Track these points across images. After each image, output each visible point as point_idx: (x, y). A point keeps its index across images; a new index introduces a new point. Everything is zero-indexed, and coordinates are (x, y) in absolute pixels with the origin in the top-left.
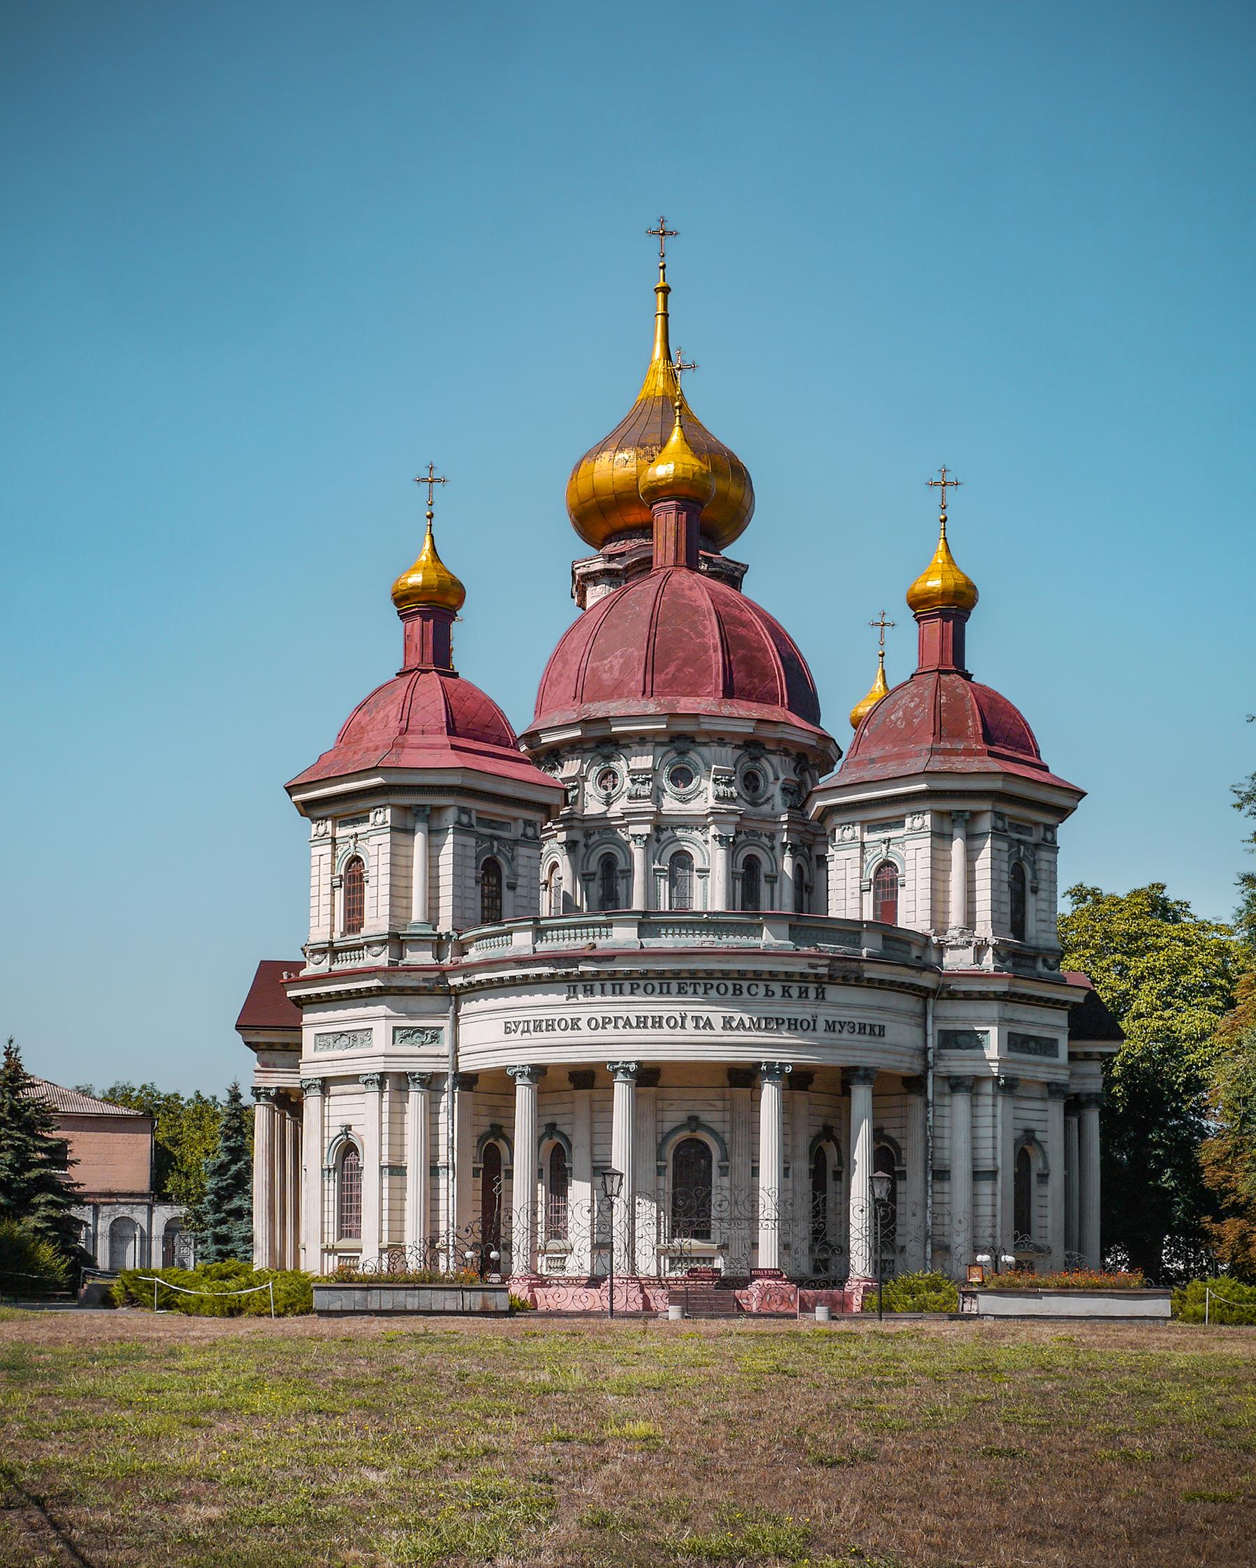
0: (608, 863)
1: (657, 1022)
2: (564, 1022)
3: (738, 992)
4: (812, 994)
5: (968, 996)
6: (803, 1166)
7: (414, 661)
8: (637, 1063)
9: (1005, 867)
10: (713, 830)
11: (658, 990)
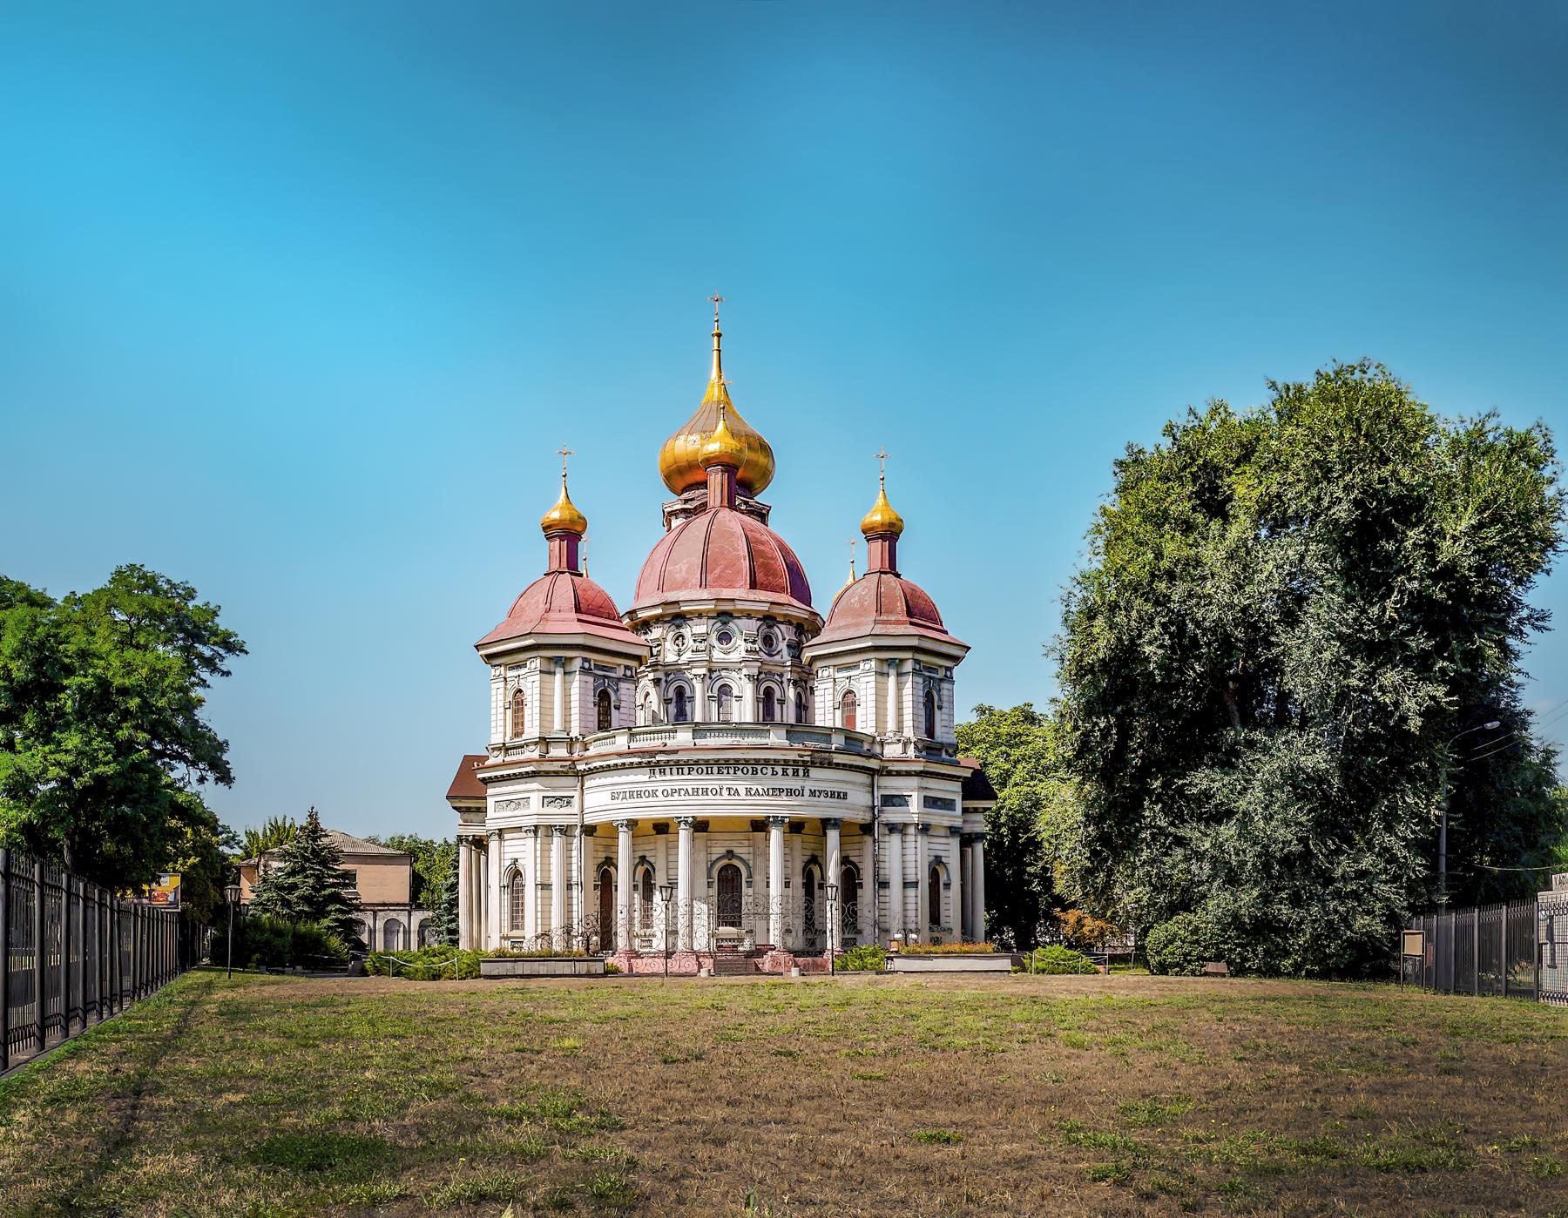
0: (680, 692)
1: (705, 792)
4: (801, 773)
5: (899, 774)
6: (798, 880)
7: (555, 566)
8: (693, 817)
9: (921, 693)
10: (745, 671)
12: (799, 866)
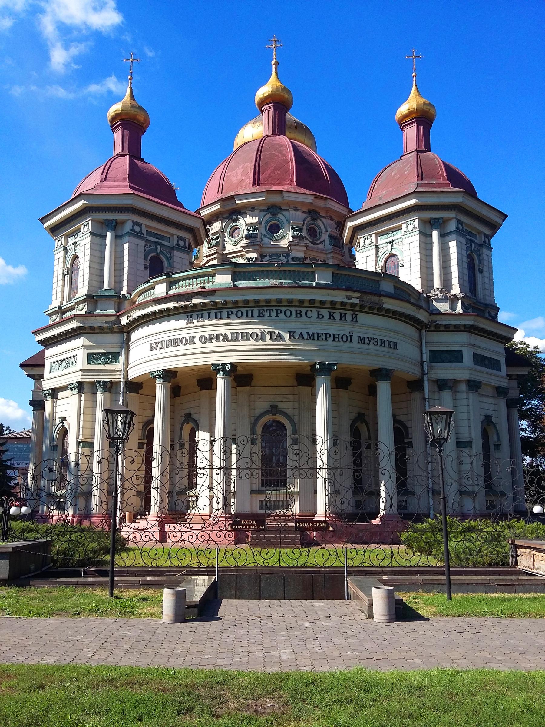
2: (184, 340)
3: (299, 315)
4: (349, 317)
5: (447, 328)
6: (346, 437)
11: (245, 315)
12: (346, 425)
